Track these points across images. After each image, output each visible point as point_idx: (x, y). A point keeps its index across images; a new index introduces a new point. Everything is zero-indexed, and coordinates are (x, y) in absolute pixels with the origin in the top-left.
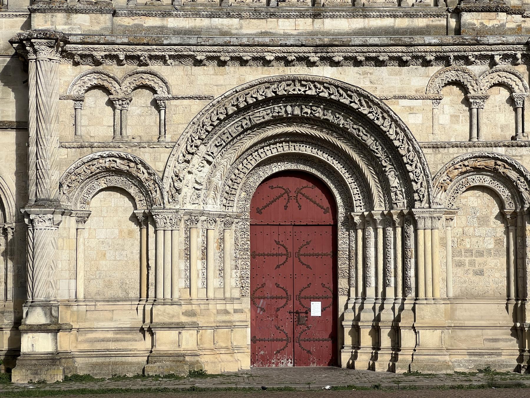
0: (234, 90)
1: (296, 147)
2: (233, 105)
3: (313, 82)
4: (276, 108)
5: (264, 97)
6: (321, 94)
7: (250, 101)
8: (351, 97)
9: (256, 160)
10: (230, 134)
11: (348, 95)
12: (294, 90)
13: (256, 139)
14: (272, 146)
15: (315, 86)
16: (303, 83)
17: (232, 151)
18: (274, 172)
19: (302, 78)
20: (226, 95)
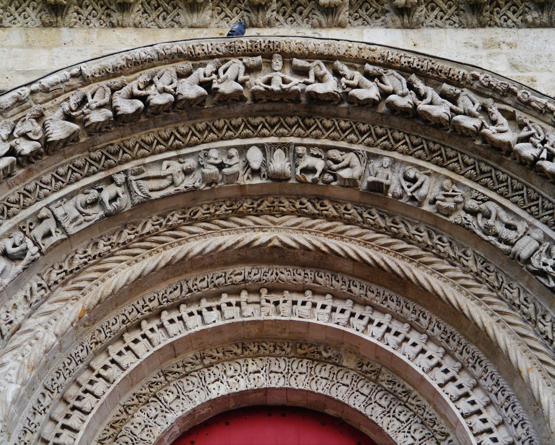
0: (75, 71)
1: (281, 305)
2: (68, 117)
3: (329, 59)
4: (214, 154)
5: (171, 97)
6: (354, 92)
7: (127, 107)
8: (453, 99)
9: (150, 341)
10: (58, 223)
11: (443, 95)
12: (269, 82)
13: (149, 263)
14: (205, 303)
15: (337, 74)
16: (298, 62)
17: (69, 294)
18: (214, 395)
19: (293, 46)
20: (46, 82)
